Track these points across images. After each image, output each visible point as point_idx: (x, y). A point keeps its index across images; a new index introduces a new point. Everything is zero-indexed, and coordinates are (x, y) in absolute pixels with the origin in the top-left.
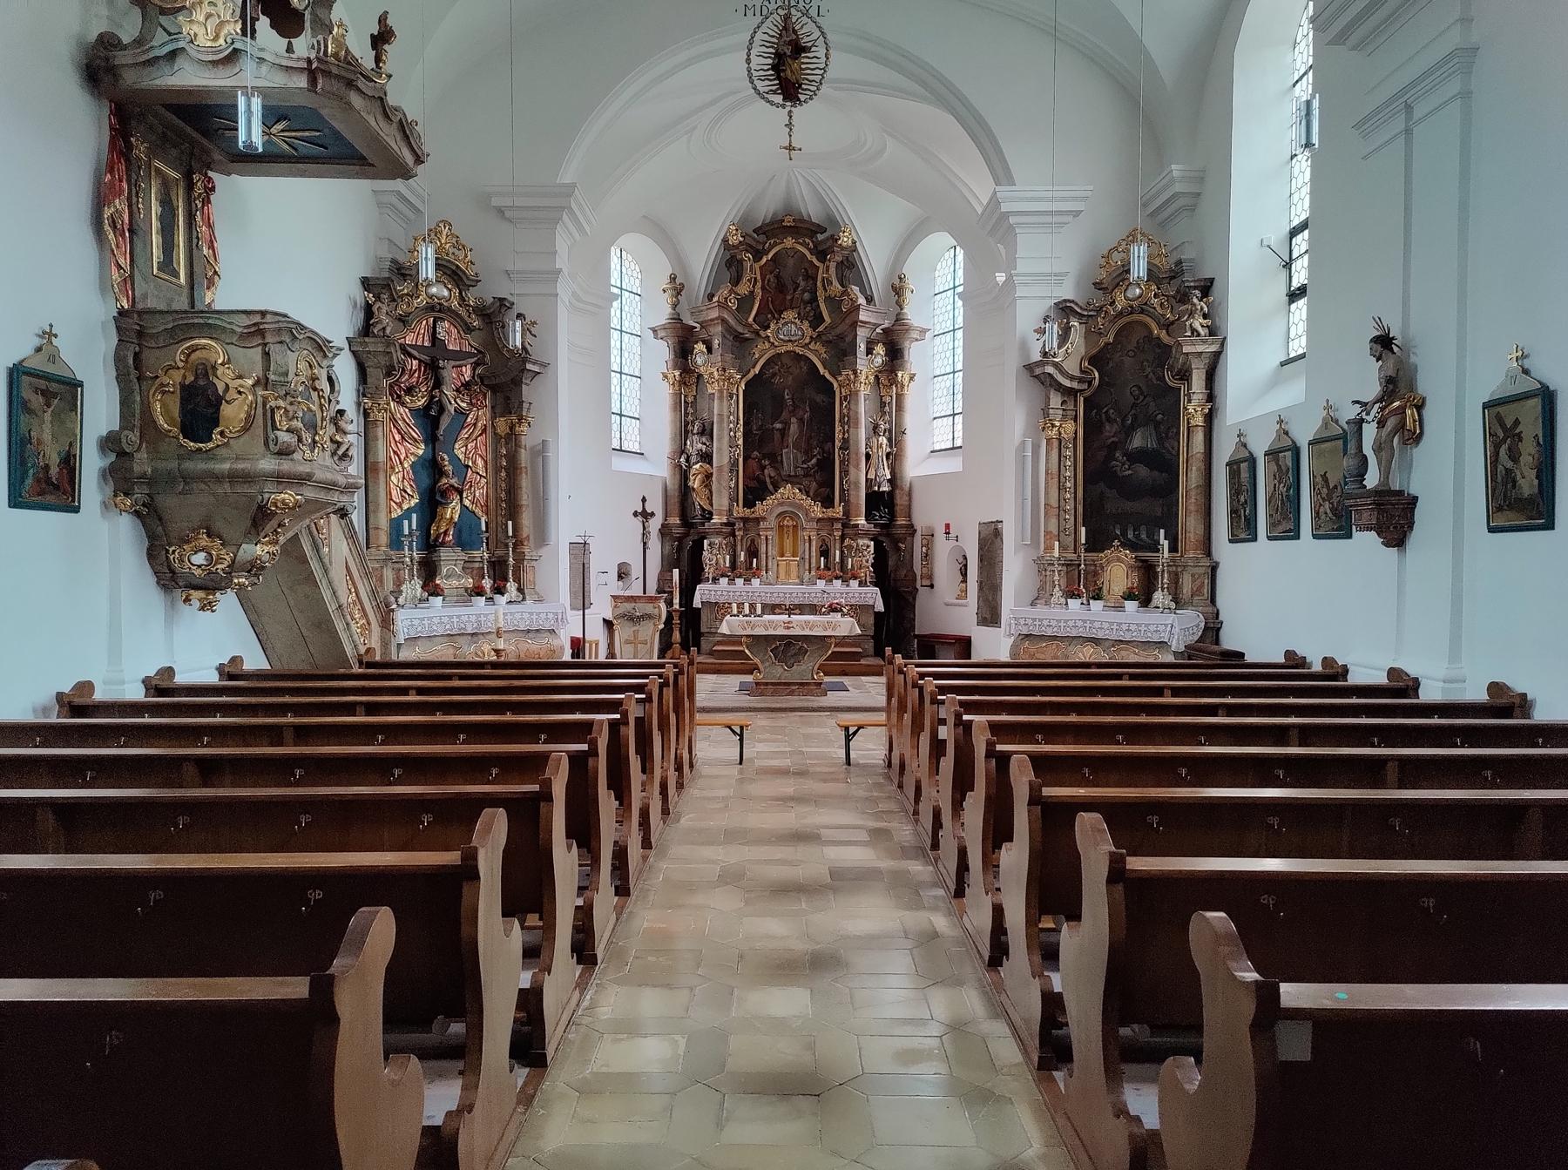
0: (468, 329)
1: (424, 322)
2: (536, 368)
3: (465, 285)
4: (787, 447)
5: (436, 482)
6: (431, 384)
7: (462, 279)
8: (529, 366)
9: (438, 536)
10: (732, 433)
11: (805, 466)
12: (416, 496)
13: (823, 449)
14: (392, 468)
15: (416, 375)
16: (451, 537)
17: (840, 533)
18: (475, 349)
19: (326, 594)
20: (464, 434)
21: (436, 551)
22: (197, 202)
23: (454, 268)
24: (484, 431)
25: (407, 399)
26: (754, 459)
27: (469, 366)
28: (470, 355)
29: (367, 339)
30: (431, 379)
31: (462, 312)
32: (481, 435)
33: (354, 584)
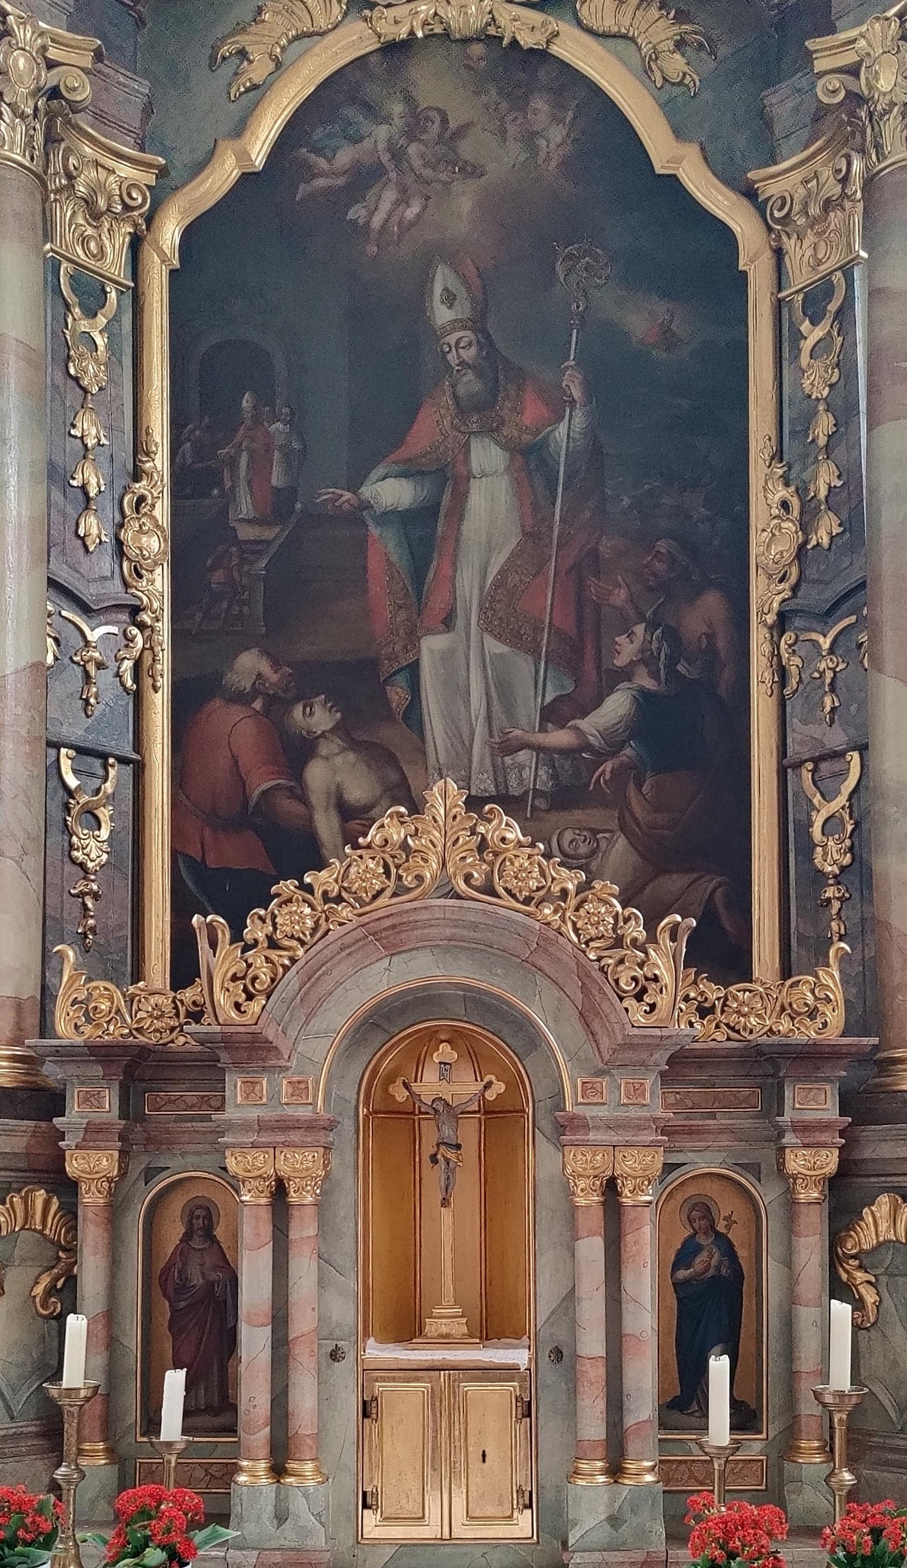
4: (448, 623)
10: (91, 525)
11: (560, 738)
13: (673, 636)
17: (830, 1161)
26: (241, 698)
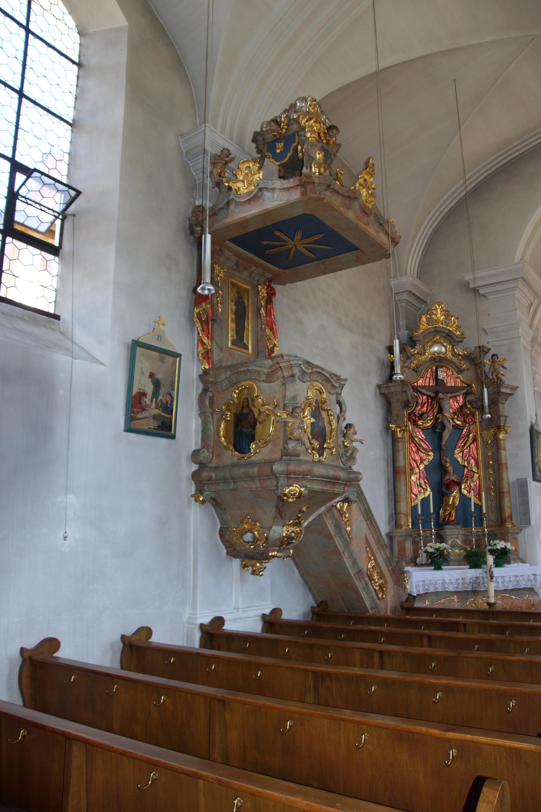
0: (460, 371)
1: (430, 370)
2: (508, 391)
3: (455, 341)
5: (442, 478)
6: (436, 411)
7: (452, 338)
8: (503, 390)
9: (445, 518)
12: (429, 489)
14: (412, 469)
15: (426, 405)
16: (454, 517)
18: (465, 383)
19: (348, 563)
20: (461, 443)
21: (443, 529)
22: (262, 302)
23: (447, 332)
24: (475, 440)
25: (420, 422)
27: (461, 396)
28: (462, 388)
29: (390, 384)
30: (436, 407)
31: (456, 360)
32: (472, 443)
33: (373, 554)
